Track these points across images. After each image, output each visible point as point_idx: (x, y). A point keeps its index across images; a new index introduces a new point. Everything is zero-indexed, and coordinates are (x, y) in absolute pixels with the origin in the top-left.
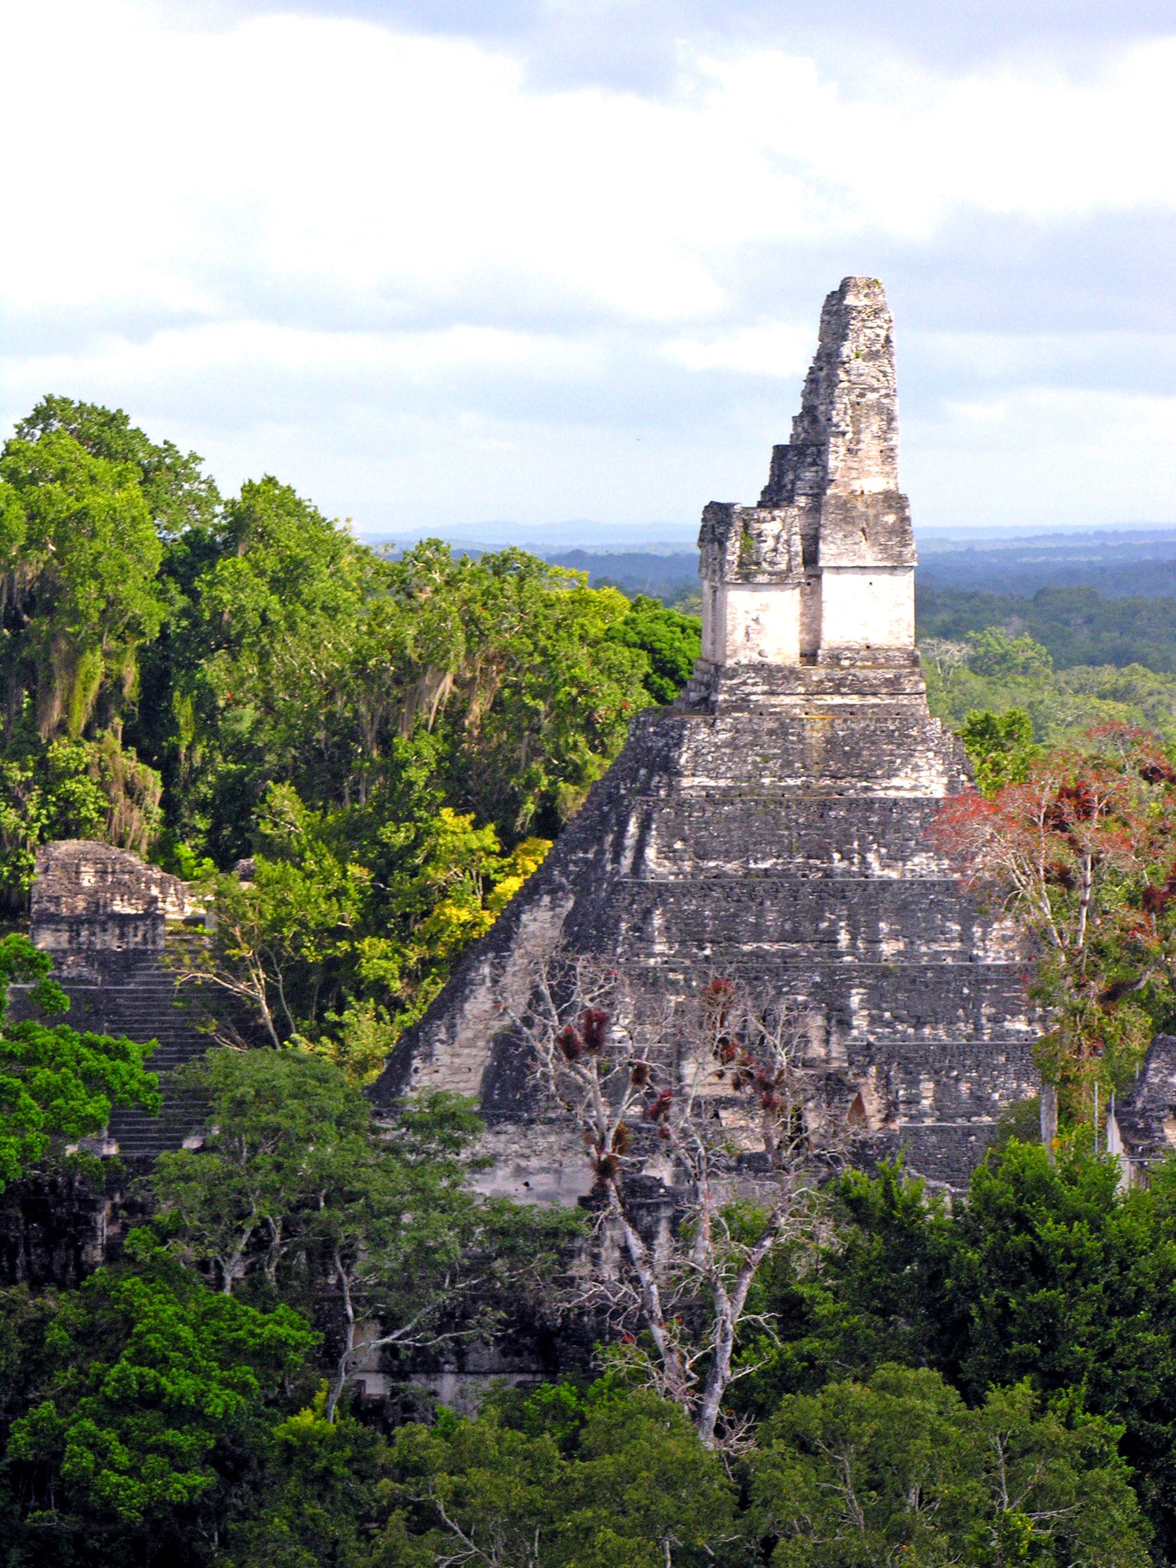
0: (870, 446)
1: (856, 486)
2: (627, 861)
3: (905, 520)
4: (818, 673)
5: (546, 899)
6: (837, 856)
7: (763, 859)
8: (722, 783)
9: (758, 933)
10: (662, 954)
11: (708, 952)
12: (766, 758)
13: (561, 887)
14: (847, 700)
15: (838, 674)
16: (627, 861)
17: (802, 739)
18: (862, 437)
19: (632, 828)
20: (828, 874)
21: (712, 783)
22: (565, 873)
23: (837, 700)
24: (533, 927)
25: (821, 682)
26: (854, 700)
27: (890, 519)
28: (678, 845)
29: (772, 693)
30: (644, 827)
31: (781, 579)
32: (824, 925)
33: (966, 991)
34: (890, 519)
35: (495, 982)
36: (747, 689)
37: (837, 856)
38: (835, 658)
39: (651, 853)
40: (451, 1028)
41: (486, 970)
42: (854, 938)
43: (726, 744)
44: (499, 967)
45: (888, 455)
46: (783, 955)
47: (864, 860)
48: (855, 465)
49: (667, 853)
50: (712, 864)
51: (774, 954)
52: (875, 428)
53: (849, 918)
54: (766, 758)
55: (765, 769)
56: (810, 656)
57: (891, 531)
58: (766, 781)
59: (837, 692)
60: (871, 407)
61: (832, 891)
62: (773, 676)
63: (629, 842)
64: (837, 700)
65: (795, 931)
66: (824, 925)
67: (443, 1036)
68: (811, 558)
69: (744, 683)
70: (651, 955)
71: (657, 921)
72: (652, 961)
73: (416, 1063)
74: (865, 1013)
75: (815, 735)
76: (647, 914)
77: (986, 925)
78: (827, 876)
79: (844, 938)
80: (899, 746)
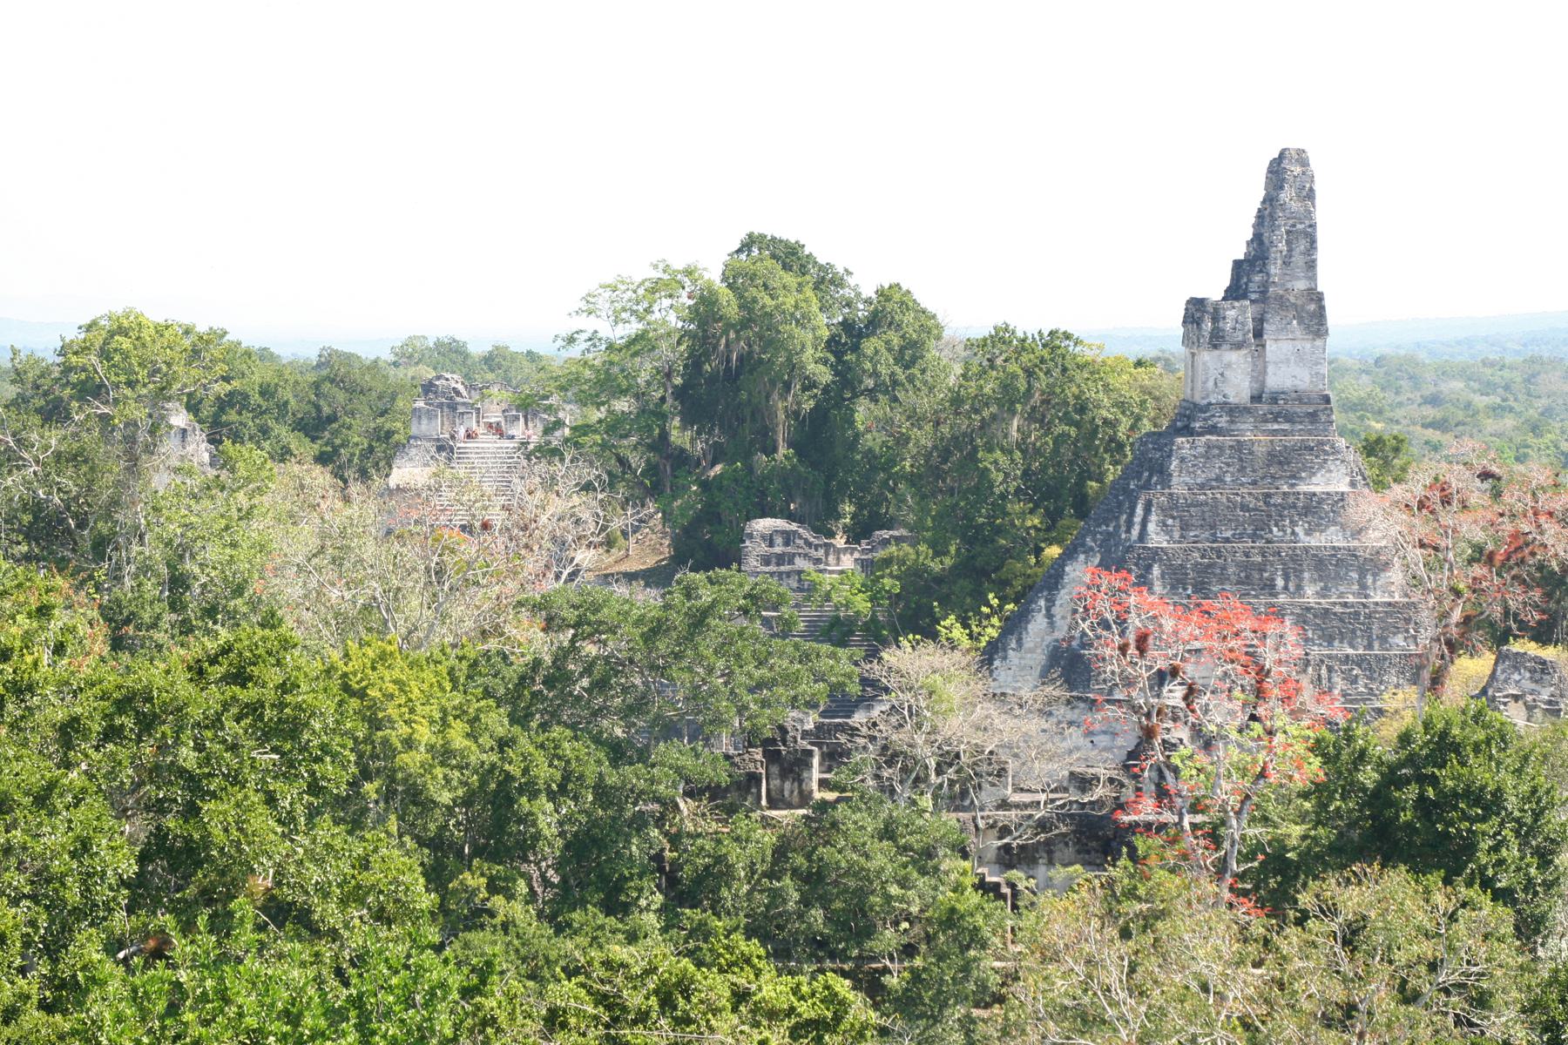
2: (1135, 532)
3: (1322, 308)
4: (1263, 408)
5: (1082, 557)
13: (1091, 549)
15: (1276, 409)
16: (1135, 532)
17: (1251, 453)
19: (1139, 511)
22: (1094, 540)
23: (1276, 427)
24: (1072, 575)
26: (1286, 426)
27: (1312, 307)
28: (1170, 522)
30: (1147, 510)
31: (1238, 346)
34: (1312, 307)
35: (1048, 609)
38: (1274, 399)
40: (1020, 641)
41: (1042, 603)
44: (1051, 602)
45: (1311, 266)
56: (1256, 398)
57: (1312, 315)
59: (1275, 420)
62: (1233, 411)
63: (1137, 519)
64: (1276, 427)
66: (1266, 575)
67: (1013, 645)
68: (1258, 334)
75: (1260, 450)
76: (1149, 568)
77: (1375, 575)
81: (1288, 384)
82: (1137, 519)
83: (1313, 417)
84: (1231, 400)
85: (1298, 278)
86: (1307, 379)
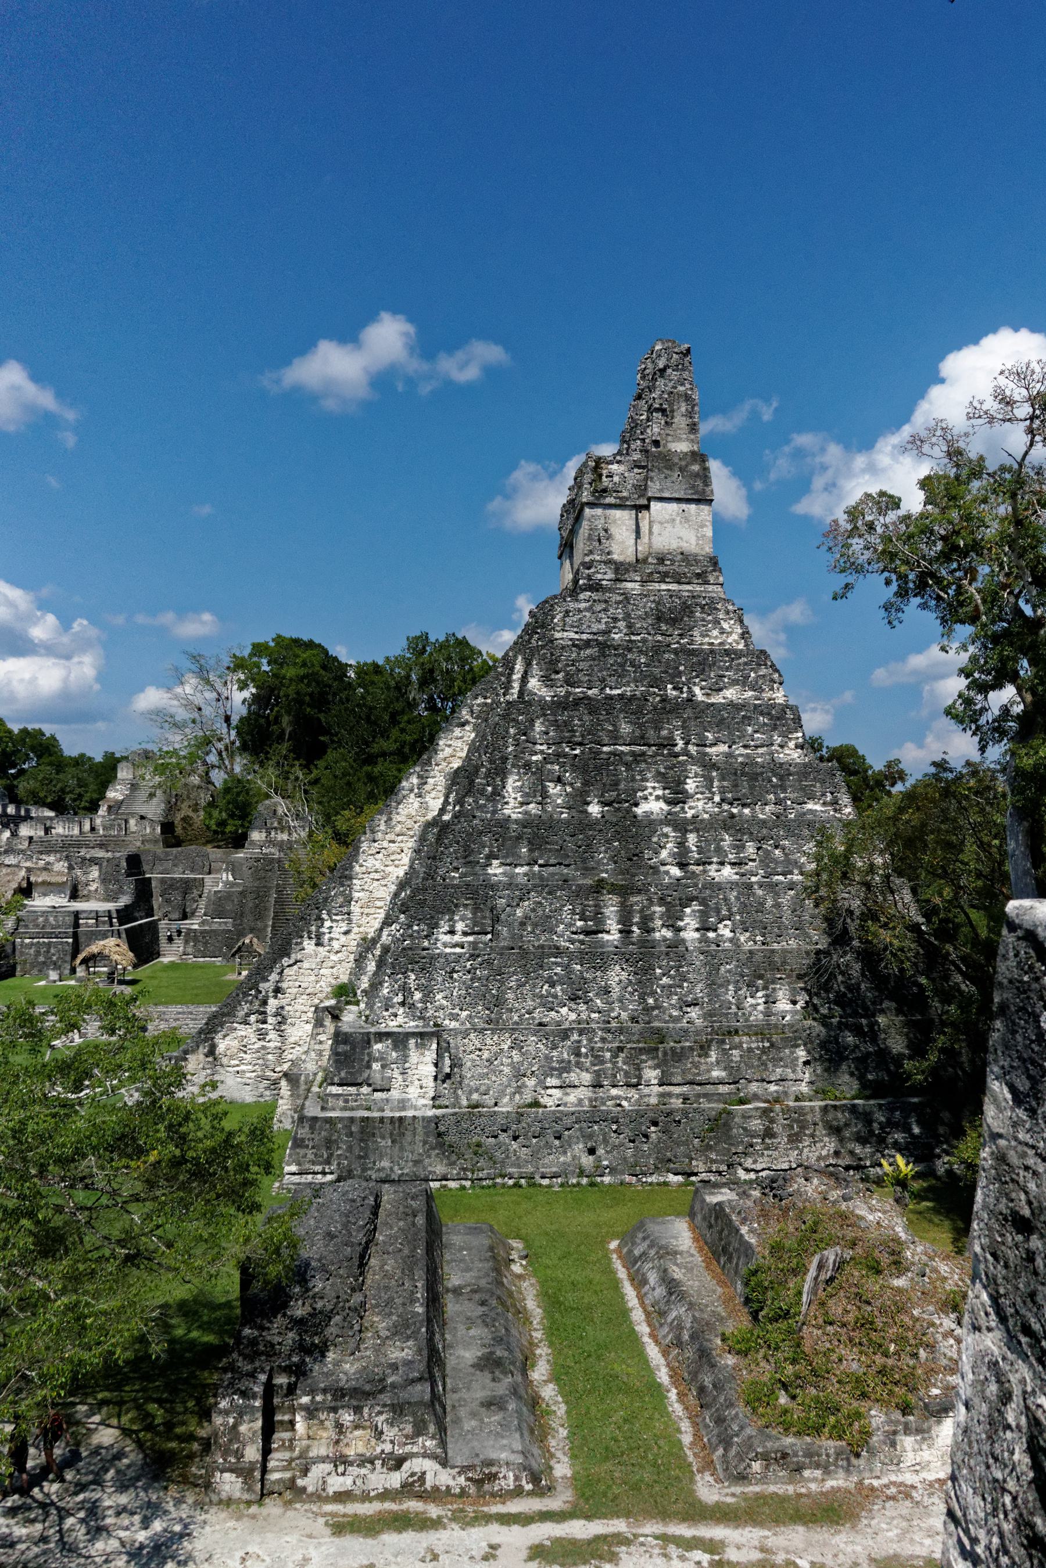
0: (680, 421)
6: (669, 686)
8: (585, 637)
9: (615, 738)
10: (542, 752)
11: (577, 752)
12: (615, 620)
13: (467, 722)
14: (670, 587)
19: (519, 667)
20: (664, 699)
21: (577, 636)
23: (664, 587)
27: (696, 468)
29: (617, 580)
30: (528, 664)
32: (664, 733)
33: (774, 780)
34: (696, 468)
36: (599, 576)
37: (669, 686)
38: (661, 560)
39: (533, 683)
41: (415, 780)
42: (687, 743)
43: (586, 609)
46: (633, 753)
47: (690, 691)
49: (547, 680)
51: (626, 754)
52: (683, 409)
53: (683, 727)
54: (615, 620)
57: (697, 475)
58: (616, 637)
60: (679, 395)
61: (669, 709)
63: (516, 676)
65: (642, 737)
66: (664, 733)
67: (383, 827)
70: (536, 753)
71: (538, 727)
72: (534, 758)
73: (364, 846)
74: (699, 796)
78: (663, 701)
79: (680, 743)
81: (674, 545)
82: (516, 676)
84: (615, 557)
85: (680, 440)
86: (693, 541)
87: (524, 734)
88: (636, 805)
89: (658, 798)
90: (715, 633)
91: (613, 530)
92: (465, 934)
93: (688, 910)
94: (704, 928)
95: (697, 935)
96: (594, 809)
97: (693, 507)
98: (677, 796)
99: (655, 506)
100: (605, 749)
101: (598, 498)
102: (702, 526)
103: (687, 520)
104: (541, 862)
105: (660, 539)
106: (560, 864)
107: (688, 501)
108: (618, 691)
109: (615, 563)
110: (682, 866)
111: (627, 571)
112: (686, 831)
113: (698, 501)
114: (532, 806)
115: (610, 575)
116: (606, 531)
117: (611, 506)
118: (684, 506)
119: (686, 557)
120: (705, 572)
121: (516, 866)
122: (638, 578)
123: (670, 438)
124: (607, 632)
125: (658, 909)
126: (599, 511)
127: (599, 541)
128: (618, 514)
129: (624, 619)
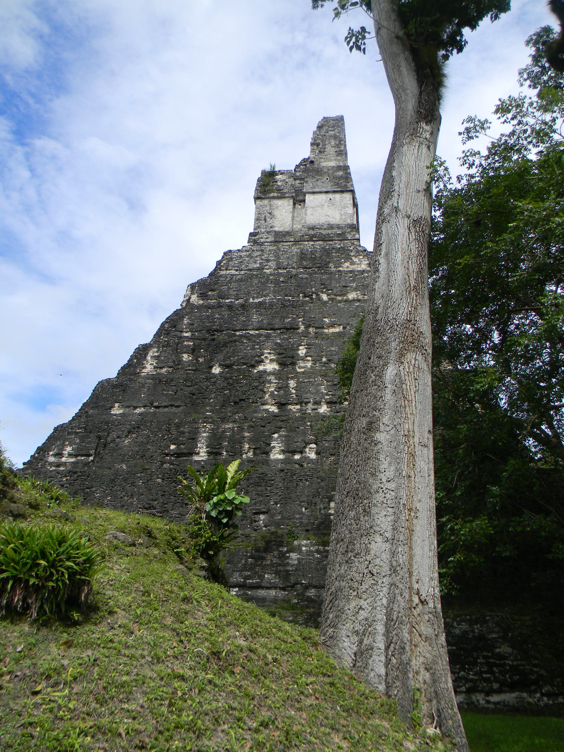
0: (330, 150)
1: (324, 164)
7: (257, 298)
18: (327, 146)
25: (303, 236)
27: (340, 173)
34: (340, 173)
36: (262, 240)
45: (342, 153)
48: (323, 157)
50: (227, 301)
52: (333, 143)
55: (266, 265)
57: (341, 178)
69: (262, 238)
80: (343, 254)
83: (342, 237)
84: (276, 229)
87: (175, 327)
88: (253, 366)
89: (272, 361)
90: (347, 264)
91: (276, 212)
92: (70, 455)
93: (276, 436)
94: (289, 451)
95: (281, 457)
96: (216, 370)
97: (338, 196)
98: (287, 360)
99: (308, 198)
100: (238, 333)
101: (265, 195)
102: (345, 207)
103: (333, 204)
104: (156, 404)
105: (312, 217)
106: (172, 406)
107: (334, 192)
108: (260, 300)
109: (275, 232)
110: (281, 405)
111: (285, 236)
112: (288, 378)
113: (342, 192)
114: (164, 370)
115: (271, 239)
116: (270, 214)
117: (274, 198)
118: (331, 196)
119: (331, 227)
120: (343, 233)
121: (135, 408)
122: (293, 240)
123: (322, 160)
124: (261, 269)
125: (247, 434)
126: (266, 202)
127: (265, 220)
128: (279, 202)
129: (274, 260)
